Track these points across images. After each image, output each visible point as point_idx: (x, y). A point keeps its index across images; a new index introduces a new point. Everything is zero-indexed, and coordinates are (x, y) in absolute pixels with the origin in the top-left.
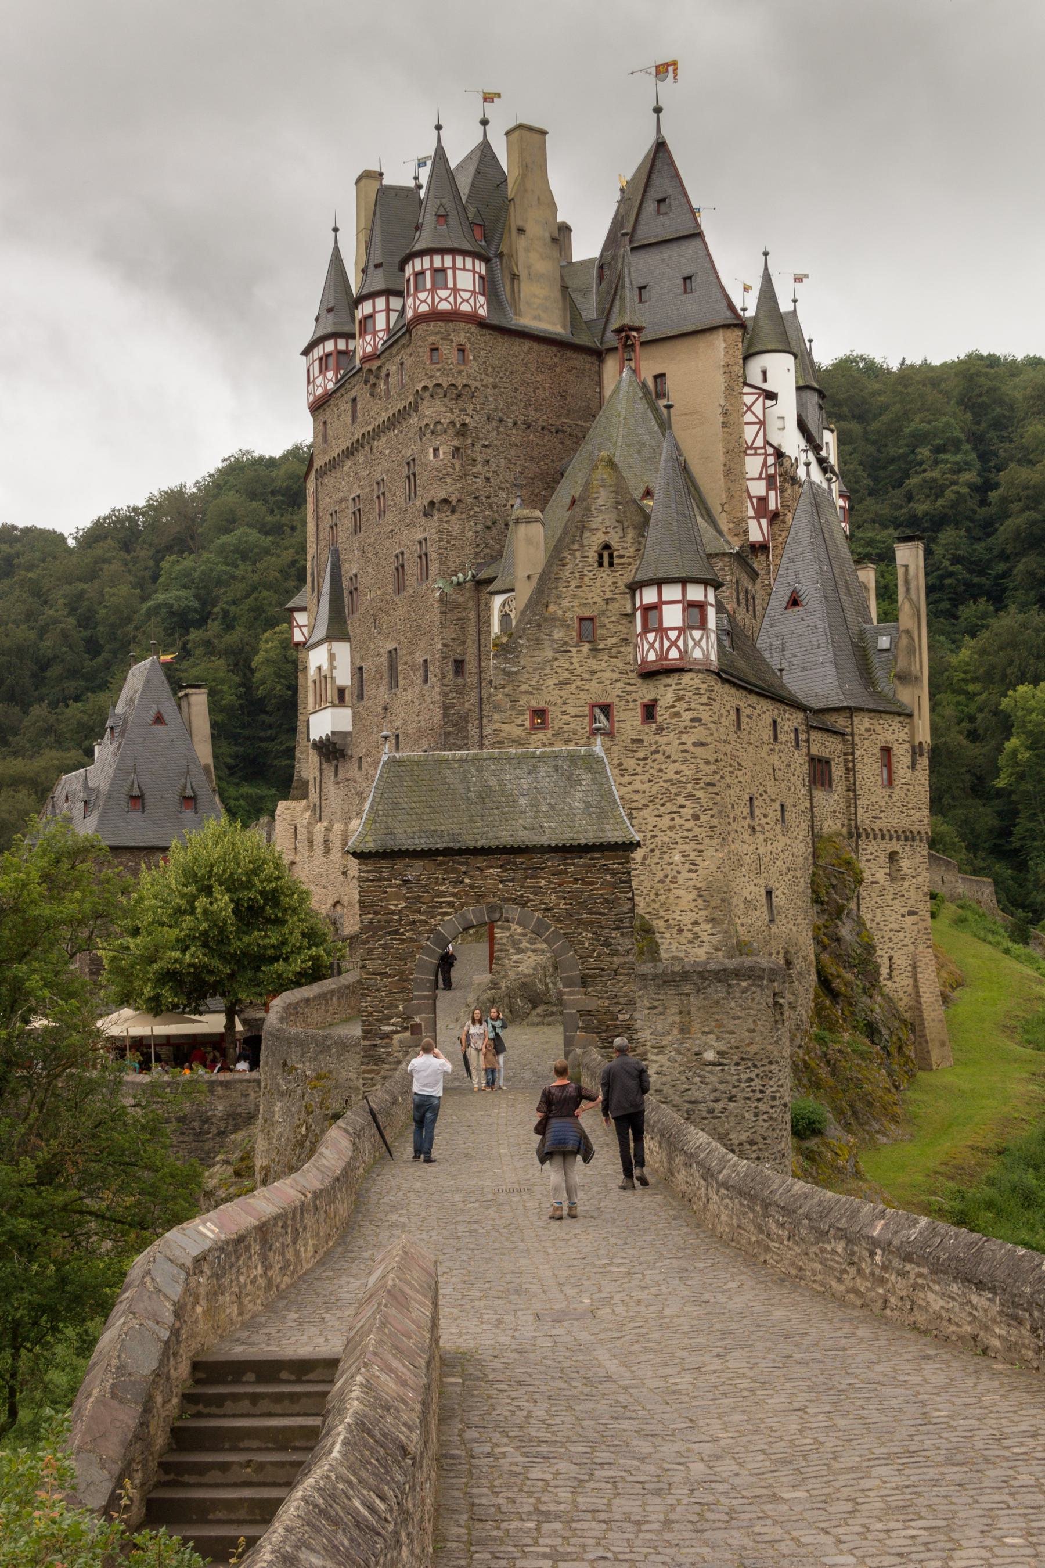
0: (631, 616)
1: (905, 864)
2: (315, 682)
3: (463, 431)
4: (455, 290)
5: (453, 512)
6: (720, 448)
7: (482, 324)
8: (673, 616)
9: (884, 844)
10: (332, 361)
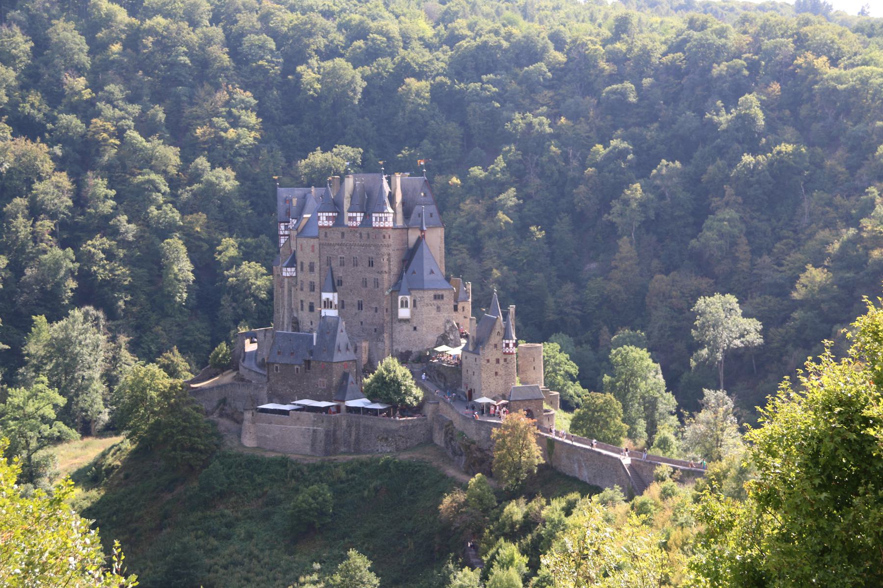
3: (389, 255)
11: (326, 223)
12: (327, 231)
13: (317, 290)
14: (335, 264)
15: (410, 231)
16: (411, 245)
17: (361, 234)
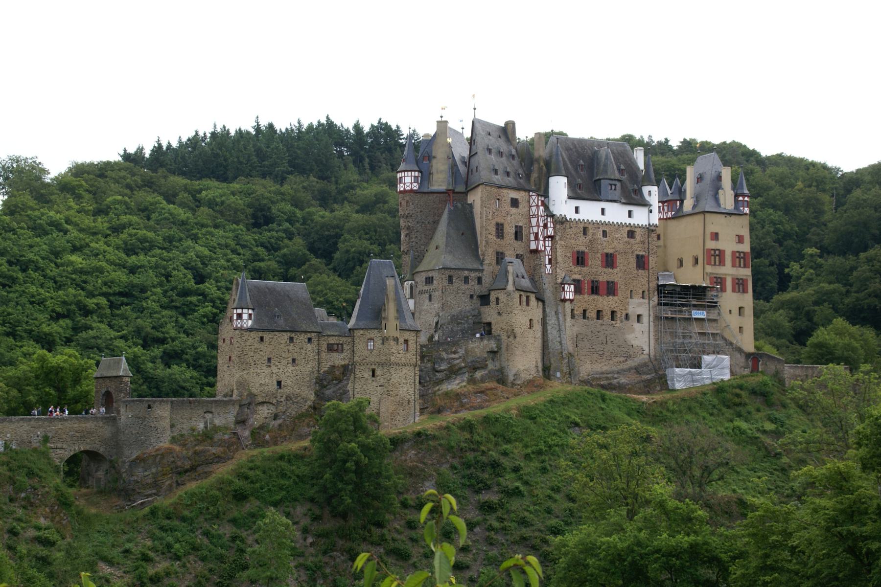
1: (378, 372)
3: (408, 228)
4: (405, 183)
5: (406, 254)
8: (235, 317)
9: (368, 366)
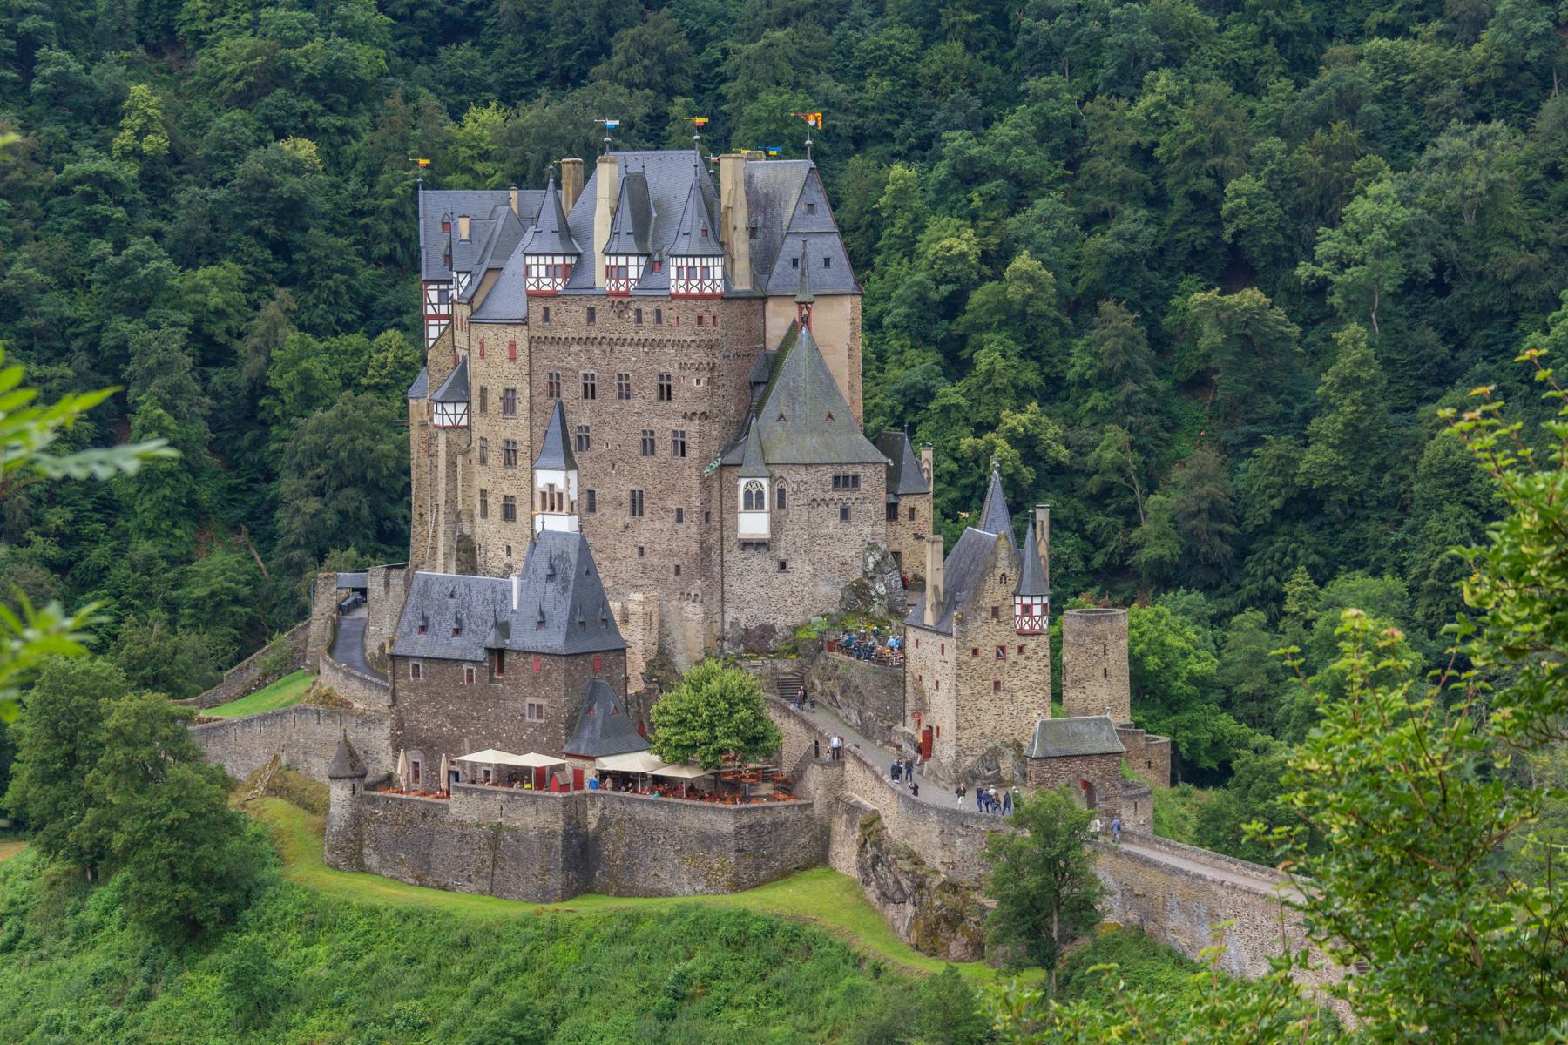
0: (1013, 607)
2: (544, 494)
3: (712, 370)
6: (846, 371)
7: (721, 297)
8: (1037, 611)
10: (559, 270)
11: (547, 285)
12: (550, 304)
13: (523, 462)
14: (571, 392)
15: (771, 305)
16: (773, 345)
17: (638, 312)
